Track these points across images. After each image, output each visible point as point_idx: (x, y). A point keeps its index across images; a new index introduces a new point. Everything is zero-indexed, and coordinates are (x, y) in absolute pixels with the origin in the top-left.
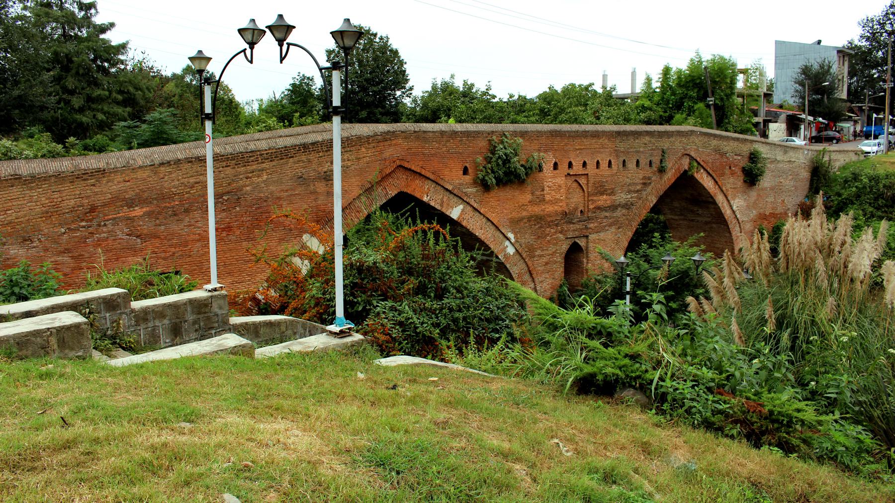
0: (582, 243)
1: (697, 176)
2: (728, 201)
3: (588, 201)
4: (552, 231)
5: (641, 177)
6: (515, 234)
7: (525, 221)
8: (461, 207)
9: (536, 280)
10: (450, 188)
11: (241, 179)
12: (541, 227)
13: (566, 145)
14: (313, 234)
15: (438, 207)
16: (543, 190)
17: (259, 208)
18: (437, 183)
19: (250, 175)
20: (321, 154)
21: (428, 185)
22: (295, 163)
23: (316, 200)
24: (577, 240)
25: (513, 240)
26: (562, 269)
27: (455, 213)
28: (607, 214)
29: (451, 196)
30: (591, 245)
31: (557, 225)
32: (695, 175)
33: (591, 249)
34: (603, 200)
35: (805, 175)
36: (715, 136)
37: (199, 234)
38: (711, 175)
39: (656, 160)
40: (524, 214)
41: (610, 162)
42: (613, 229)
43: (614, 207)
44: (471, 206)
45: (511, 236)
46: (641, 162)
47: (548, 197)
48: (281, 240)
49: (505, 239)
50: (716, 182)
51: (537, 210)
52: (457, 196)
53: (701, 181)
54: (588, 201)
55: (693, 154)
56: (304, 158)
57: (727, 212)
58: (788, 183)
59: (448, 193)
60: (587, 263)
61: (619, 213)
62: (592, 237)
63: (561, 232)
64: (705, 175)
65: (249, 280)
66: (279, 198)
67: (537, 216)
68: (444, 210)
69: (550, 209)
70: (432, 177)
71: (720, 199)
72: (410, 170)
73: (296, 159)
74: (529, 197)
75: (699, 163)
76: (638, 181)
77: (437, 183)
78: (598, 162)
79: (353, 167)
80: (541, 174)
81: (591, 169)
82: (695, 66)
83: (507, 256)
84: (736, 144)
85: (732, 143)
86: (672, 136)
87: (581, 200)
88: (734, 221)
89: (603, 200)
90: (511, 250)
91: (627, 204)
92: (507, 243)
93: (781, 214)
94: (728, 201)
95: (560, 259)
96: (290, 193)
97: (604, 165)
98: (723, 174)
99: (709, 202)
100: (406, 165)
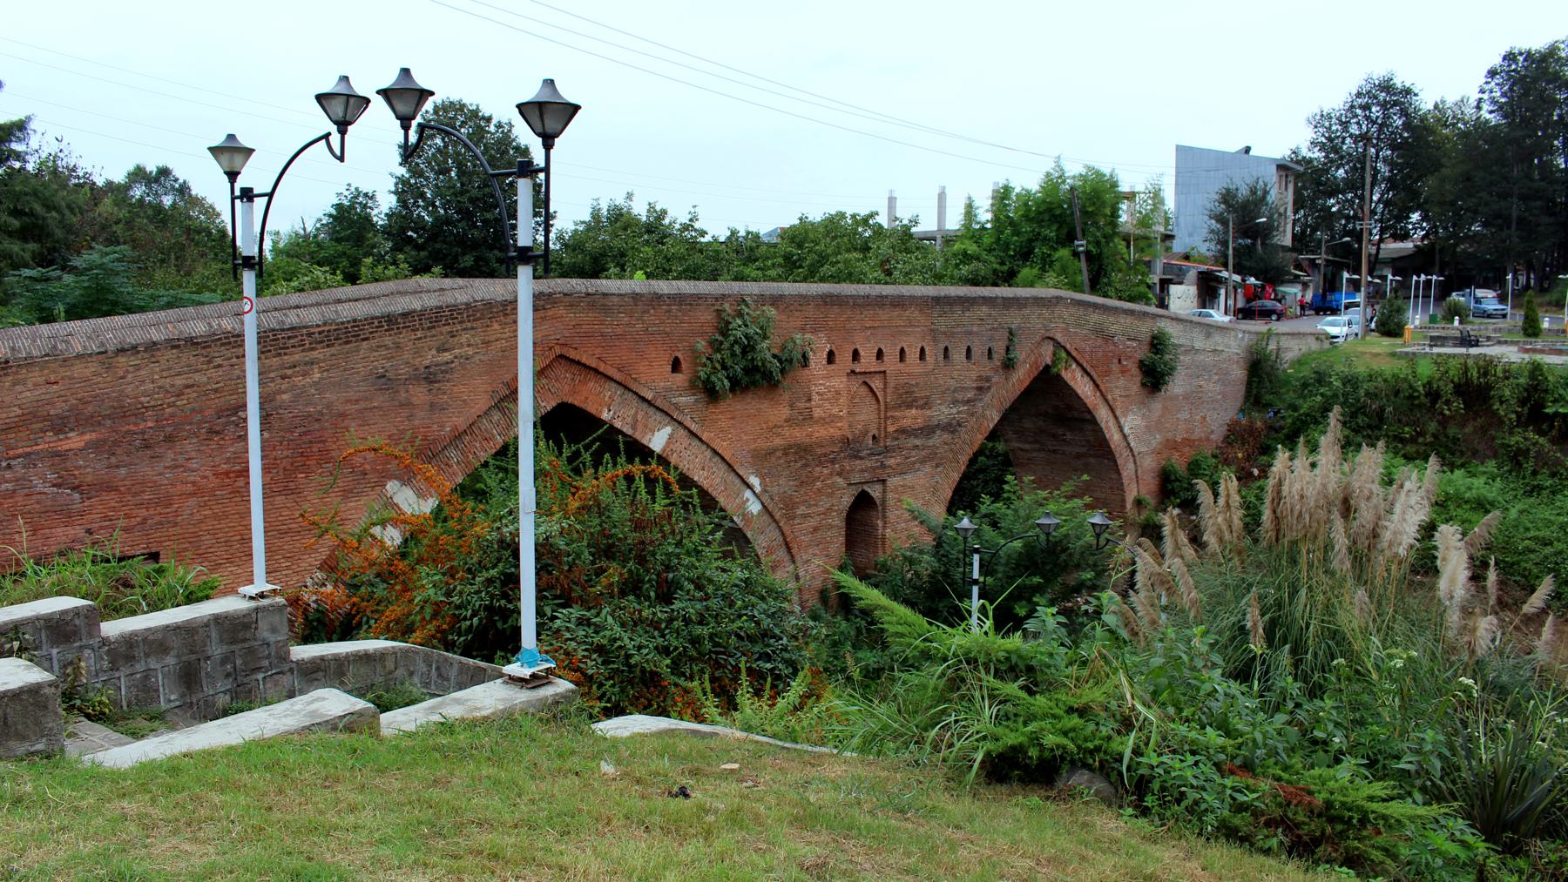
0: (875, 492)
1: (1066, 376)
2: (1116, 418)
3: (886, 418)
4: (826, 471)
6: (762, 477)
7: (779, 454)
8: (668, 429)
9: (797, 558)
10: (649, 396)
11: (273, 380)
12: (806, 465)
13: (849, 320)
14: (407, 478)
15: (627, 430)
16: (810, 400)
17: (305, 433)
18: (626, 388)
19: (289, 372)
20: (419, 334)
21: (610, 391)
22: (372, 350)
23: (410, 418)
24: (866, 488)
25: (758, 489)
26: (842, 539)
27: (657, 441)
28: (918, 442)
29: (651, 411)
30: (890, 495)
31: (833, 462)
32: (1063, 373)
33: (891, 502)
34: (912, 417)
35: (1239, 373)
36: (1095, 306)
37: (194, 483)
38: (1088, 374)
39: (999, 348)
40: (778, 442)
41: (922, 350)
42: (928, 468)
43: (928, 430)
44: (686, 428)
45: (755, 481)
46: (974, 350)
47: (817, 413)
48: (347, 494)
49: (743, 487)
50: (1097, 386)
51: (799, 435)
52: (662, 411)
53: (1072, 384)
54: (886, 418)
55: (1059, 337)
56: (388, 340)
57: (1114, 437)
58: (1212, 387)
59: (645, 405)
60: (884, 528)
61: (938, 439)
62: (893, 482)
63: (839, 474)
64: (1079, 374)
65: (288, 568)
66: (343, 415)
67: (798, 446)
68: (638, 436)
69: (821, 432)
70: (617, 376)
71: (1102, 414)
72: (579, 363)
73: (373, 343)
74: (785, 412)
75: (1069, 353)
76: (969, 384)
77: (626, 388)
78: (902, 351)
79: (477, 358)
80: (806, 371)
81: (891, 363)
82: (1052, 183)
83: (747, 517)
84: (1129, 320)
85: (1122, 319)
86: (1025, 306)
87: (874, 416)
88: (1126, 453)
89: (912, 417)
90: (754, 507)
91: (950, 424)
92: (748, 494)
93: (1200, 440)
94: (1116, 418)
95: (838, 521)
96: (362, 405)
98: (1108, 373)
99: (1084, 421)
100: (572, 354)
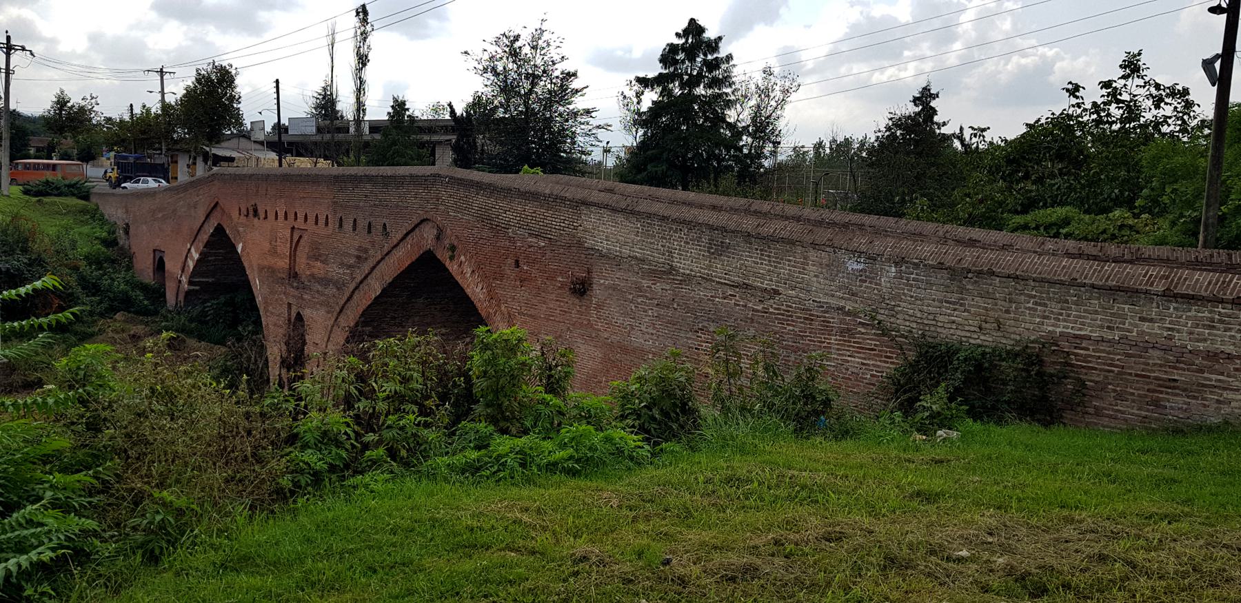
5: (357, 244)
36: (479, 186)
61: (331, 290)
97: (322, 221)
